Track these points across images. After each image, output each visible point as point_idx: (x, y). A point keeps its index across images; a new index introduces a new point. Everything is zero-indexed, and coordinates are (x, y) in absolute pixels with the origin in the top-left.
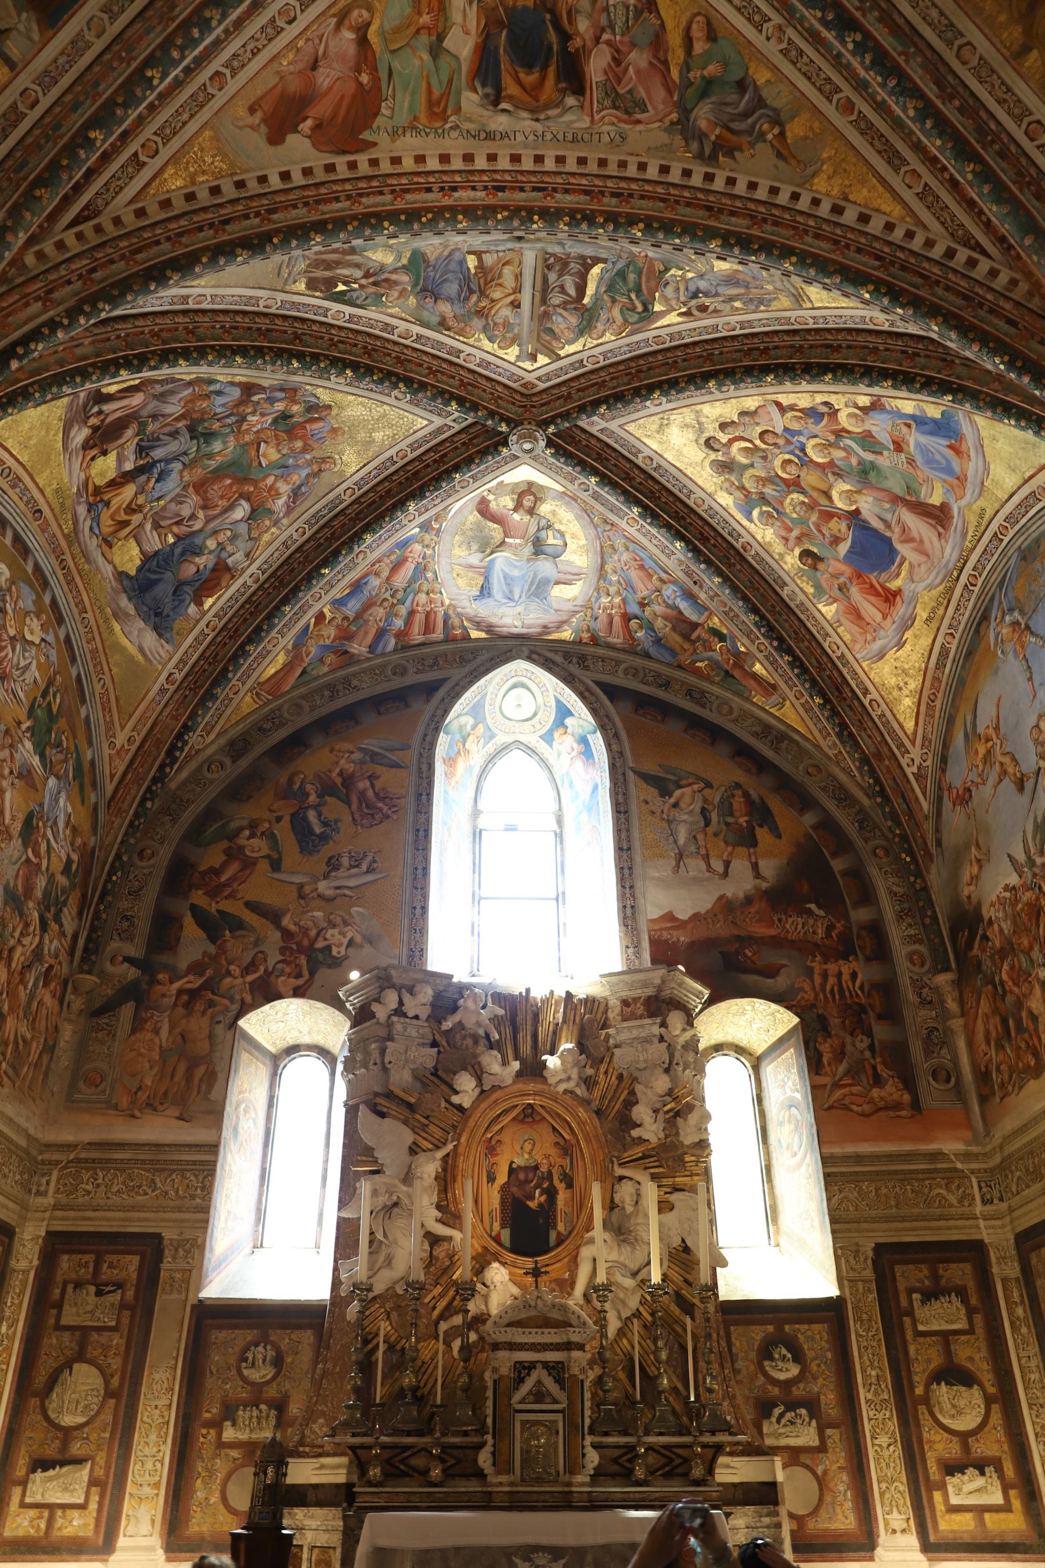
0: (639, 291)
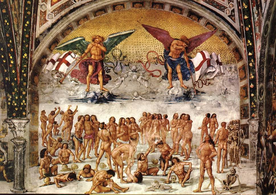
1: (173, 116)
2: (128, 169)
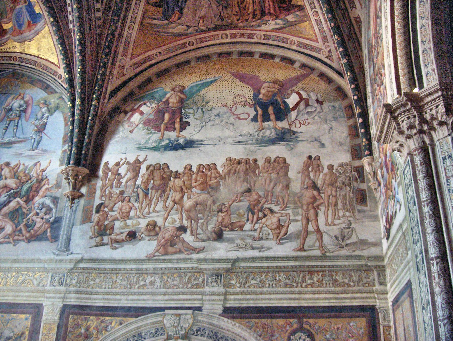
2: (205, 224)
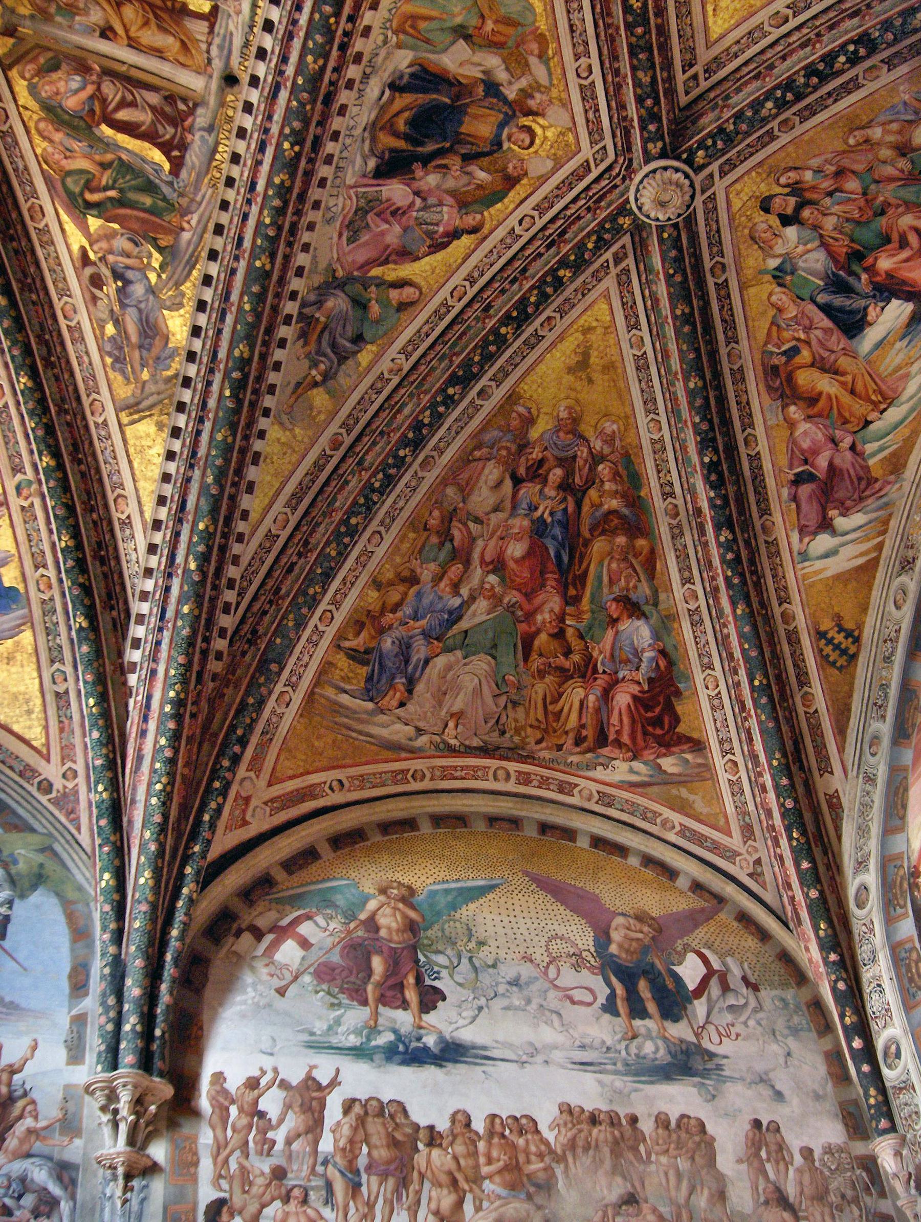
0: (121, 202)
1: (653, 1119)
